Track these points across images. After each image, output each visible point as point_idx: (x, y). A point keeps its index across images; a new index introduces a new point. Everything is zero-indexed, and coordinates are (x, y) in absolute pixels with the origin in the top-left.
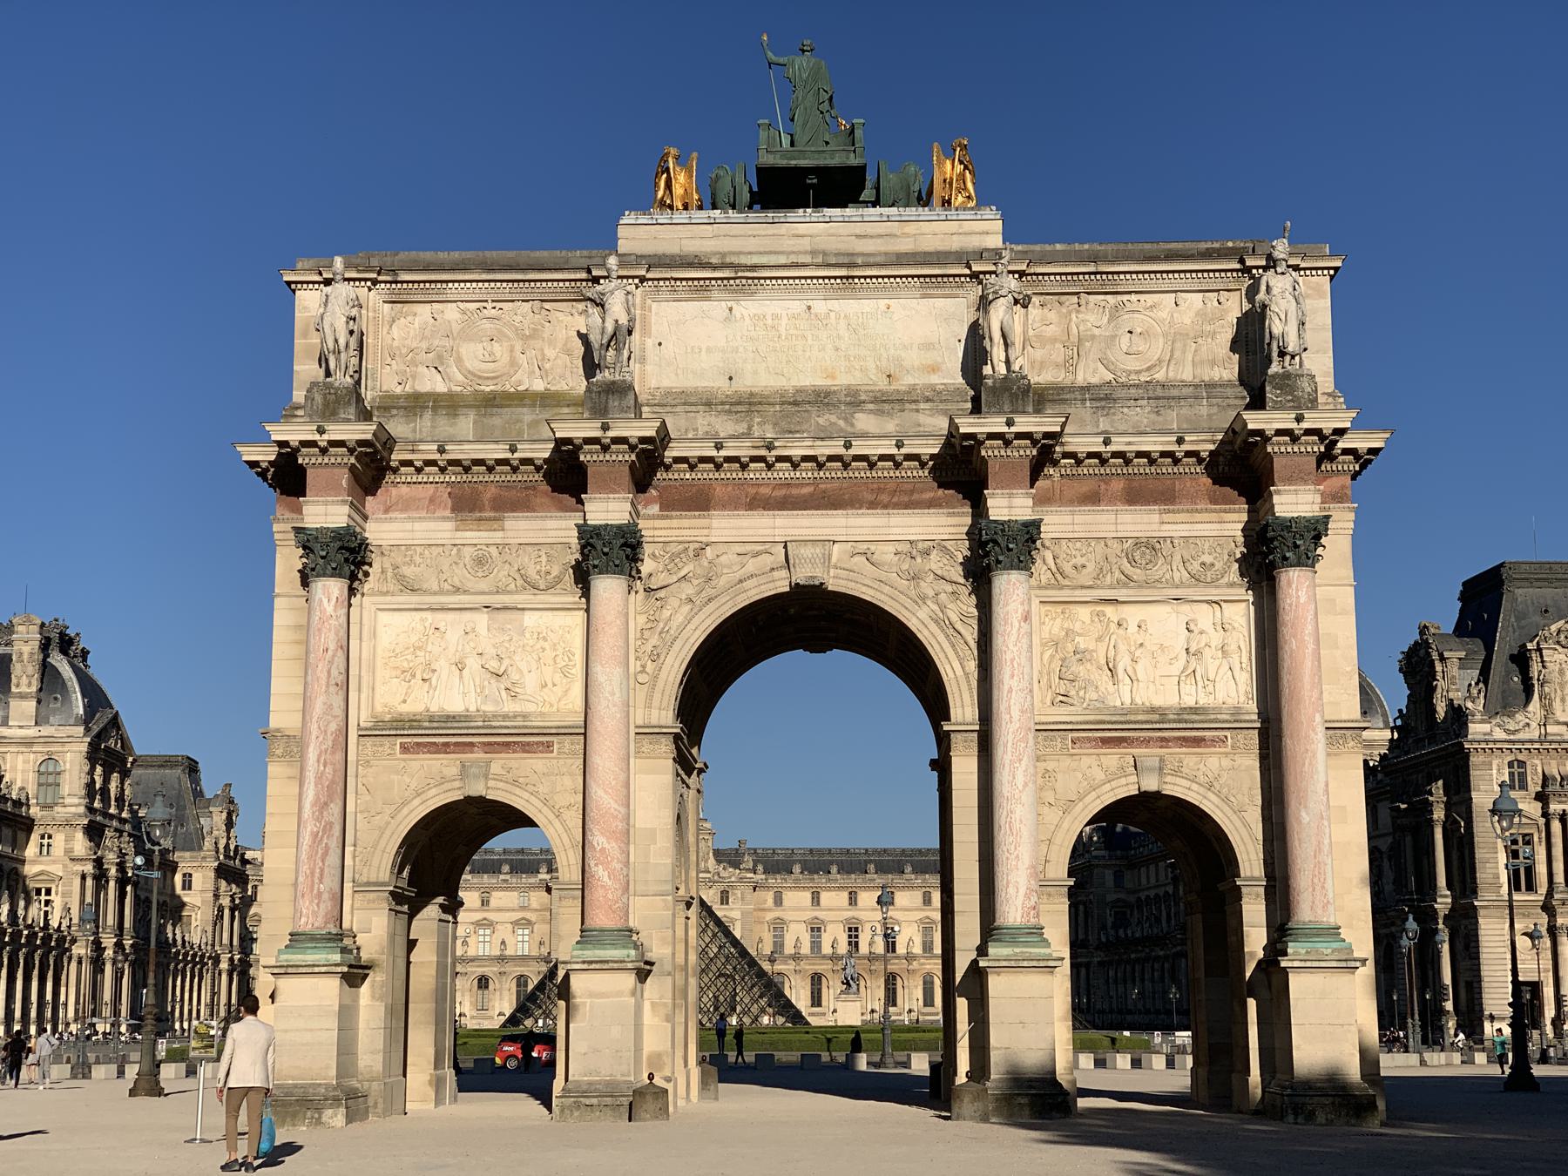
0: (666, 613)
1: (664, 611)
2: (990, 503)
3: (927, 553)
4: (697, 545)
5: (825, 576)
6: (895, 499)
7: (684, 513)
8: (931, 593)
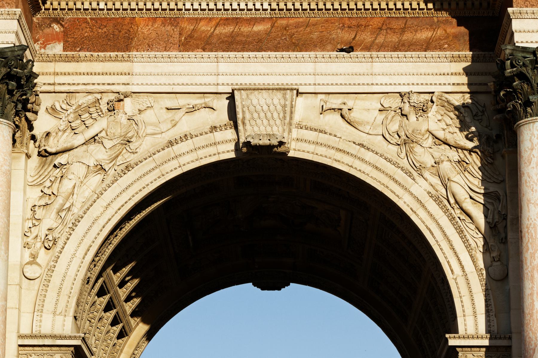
0: (67, 185)
1: (65, 181)
2: (516, 25)
3: (423, 110)
4: (112, 97)
5: (286, 135)
6: (380, 39)
7: (95, 54)
8: (430, 162)
